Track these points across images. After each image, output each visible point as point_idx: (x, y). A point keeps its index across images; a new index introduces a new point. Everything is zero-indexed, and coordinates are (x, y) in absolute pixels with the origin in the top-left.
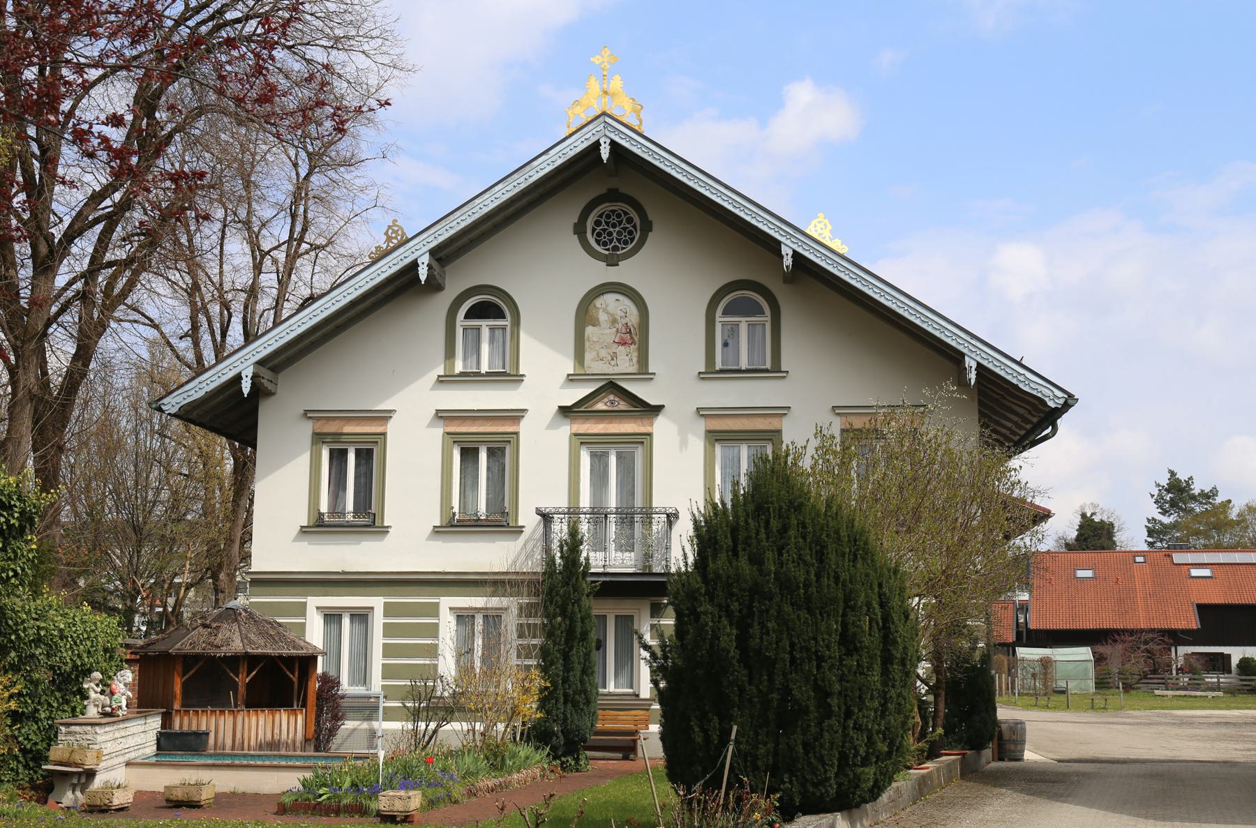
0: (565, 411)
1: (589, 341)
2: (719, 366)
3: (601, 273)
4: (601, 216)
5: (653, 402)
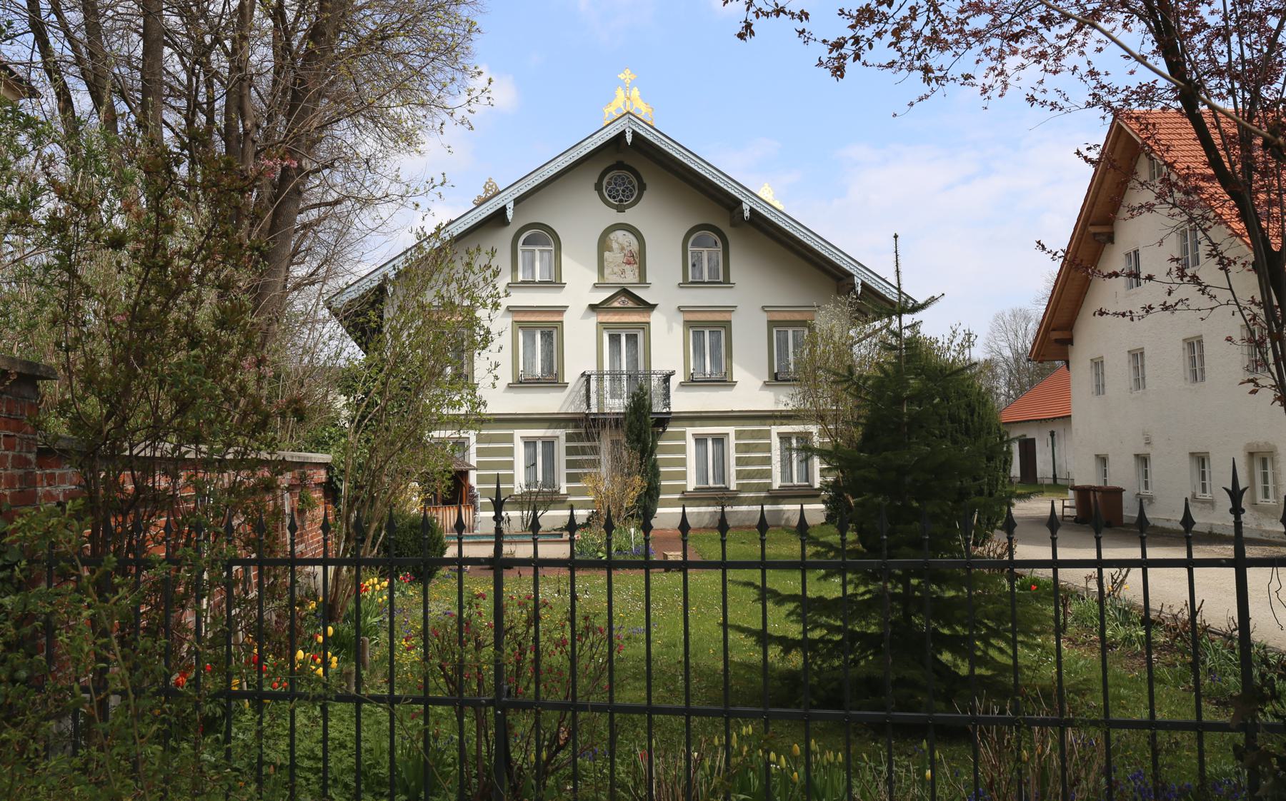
0: (593, 308)
2: (690, 279)
3: (614, 217)
4: (611, 179)
5: (652, 302)
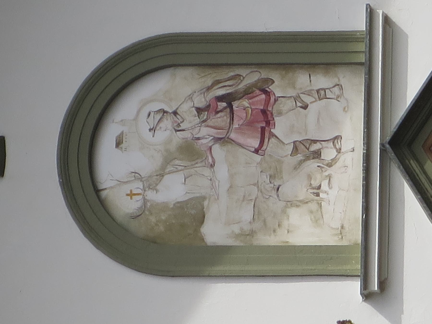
1: (252, 233)
